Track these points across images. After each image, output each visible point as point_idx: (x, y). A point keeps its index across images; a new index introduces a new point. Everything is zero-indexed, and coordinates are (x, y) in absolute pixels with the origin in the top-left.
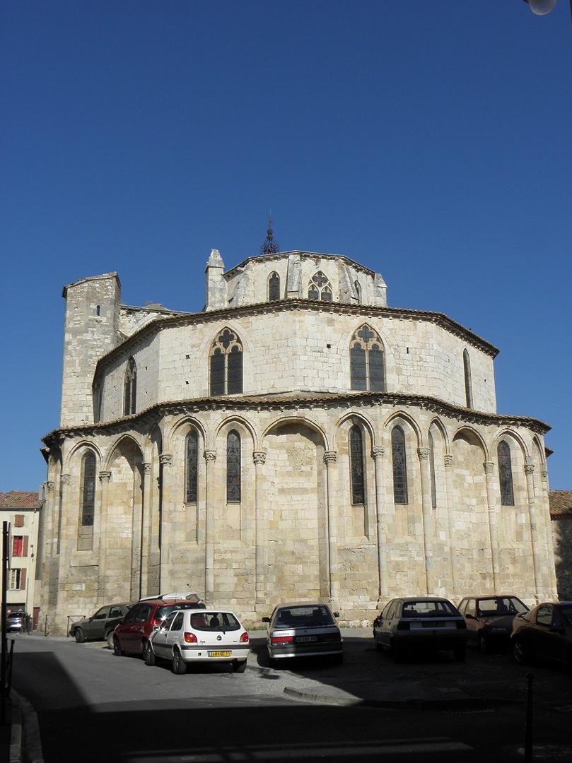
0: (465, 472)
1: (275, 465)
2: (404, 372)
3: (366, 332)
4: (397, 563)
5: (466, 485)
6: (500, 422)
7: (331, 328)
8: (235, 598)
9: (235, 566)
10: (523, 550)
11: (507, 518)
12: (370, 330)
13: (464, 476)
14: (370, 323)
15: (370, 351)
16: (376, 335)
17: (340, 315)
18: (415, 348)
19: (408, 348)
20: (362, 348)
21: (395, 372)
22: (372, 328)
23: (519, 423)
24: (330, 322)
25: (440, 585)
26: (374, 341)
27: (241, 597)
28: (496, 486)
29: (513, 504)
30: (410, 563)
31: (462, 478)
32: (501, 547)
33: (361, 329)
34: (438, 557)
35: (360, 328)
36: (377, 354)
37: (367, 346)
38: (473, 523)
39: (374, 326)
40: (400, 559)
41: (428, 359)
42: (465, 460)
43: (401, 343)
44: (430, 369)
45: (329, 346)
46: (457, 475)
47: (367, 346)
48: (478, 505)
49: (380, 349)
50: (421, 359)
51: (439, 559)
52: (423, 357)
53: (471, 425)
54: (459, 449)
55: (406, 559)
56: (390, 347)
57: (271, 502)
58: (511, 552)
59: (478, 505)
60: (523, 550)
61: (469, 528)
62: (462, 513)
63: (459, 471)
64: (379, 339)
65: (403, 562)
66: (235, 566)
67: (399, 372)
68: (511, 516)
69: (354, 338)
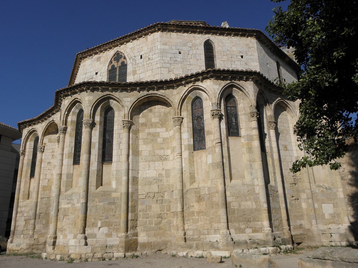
0: (158, 130)
1: (53, 152)
2: (138, 72)
3: (118, 56)
4: (65, 209)
5: (160, 140)
6: (183, 82)
7: (99, 62)
8: (23, 234)
9: (25, 215)
10: (209, 188)
11: (199, 161)
12: (120, 54)
13: (159, 133)
14: (119, 50)
15: (120, 67)
16: (123, 56)
17: (104, 52)
18: (146, 54)
19: (141, 56)
20: (115, 67)
21: (132, 74)
22: (121, 53)
23: (200, 77)
24: (98, 59)
25: (99, 224)
26: (122, 59)
27: (25, 233)
28: (187, 136)
29: (205, 148)
30: (72, 209)
31: (156, 135)
32: (188, 186)
33: (116, 56)
34: (100, 202)
35: (115, 55)
36: (124, 66)
37: (116, 65)
38: (166, 170)
39: (122, 51)
40: (67, 206)
41: (154, 57)
42: (160, 120)
43: (136, 54)
44: (155, 63)
45: (97, 73)
46: (149, 134)
47: (116, 65)
48: (171, 154)
49: (125, 63)
50: (149, 59)
51: (102, 204)
52: (150, 57)
53: (155, 92)
54: (154, 113)
55: (70, 206)
56: (130, 59)
57: (46, 174)
58: (197, 191)
59: (171, 154)
60: (209, 188)
61: (160, 175)
62: (151, 163)
63: (152, 130)
64: (125, 58)
65: (69, 208)
66: (25, 215)
67: (134, 73)
68: (202, 159)
69: (111, 62)
